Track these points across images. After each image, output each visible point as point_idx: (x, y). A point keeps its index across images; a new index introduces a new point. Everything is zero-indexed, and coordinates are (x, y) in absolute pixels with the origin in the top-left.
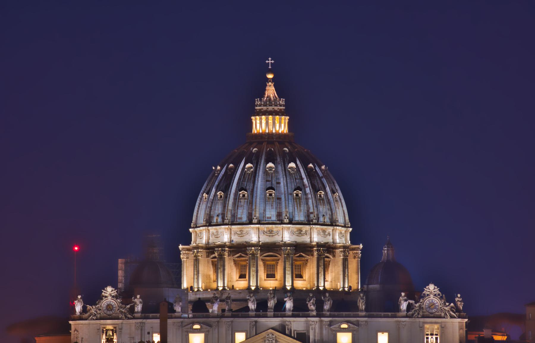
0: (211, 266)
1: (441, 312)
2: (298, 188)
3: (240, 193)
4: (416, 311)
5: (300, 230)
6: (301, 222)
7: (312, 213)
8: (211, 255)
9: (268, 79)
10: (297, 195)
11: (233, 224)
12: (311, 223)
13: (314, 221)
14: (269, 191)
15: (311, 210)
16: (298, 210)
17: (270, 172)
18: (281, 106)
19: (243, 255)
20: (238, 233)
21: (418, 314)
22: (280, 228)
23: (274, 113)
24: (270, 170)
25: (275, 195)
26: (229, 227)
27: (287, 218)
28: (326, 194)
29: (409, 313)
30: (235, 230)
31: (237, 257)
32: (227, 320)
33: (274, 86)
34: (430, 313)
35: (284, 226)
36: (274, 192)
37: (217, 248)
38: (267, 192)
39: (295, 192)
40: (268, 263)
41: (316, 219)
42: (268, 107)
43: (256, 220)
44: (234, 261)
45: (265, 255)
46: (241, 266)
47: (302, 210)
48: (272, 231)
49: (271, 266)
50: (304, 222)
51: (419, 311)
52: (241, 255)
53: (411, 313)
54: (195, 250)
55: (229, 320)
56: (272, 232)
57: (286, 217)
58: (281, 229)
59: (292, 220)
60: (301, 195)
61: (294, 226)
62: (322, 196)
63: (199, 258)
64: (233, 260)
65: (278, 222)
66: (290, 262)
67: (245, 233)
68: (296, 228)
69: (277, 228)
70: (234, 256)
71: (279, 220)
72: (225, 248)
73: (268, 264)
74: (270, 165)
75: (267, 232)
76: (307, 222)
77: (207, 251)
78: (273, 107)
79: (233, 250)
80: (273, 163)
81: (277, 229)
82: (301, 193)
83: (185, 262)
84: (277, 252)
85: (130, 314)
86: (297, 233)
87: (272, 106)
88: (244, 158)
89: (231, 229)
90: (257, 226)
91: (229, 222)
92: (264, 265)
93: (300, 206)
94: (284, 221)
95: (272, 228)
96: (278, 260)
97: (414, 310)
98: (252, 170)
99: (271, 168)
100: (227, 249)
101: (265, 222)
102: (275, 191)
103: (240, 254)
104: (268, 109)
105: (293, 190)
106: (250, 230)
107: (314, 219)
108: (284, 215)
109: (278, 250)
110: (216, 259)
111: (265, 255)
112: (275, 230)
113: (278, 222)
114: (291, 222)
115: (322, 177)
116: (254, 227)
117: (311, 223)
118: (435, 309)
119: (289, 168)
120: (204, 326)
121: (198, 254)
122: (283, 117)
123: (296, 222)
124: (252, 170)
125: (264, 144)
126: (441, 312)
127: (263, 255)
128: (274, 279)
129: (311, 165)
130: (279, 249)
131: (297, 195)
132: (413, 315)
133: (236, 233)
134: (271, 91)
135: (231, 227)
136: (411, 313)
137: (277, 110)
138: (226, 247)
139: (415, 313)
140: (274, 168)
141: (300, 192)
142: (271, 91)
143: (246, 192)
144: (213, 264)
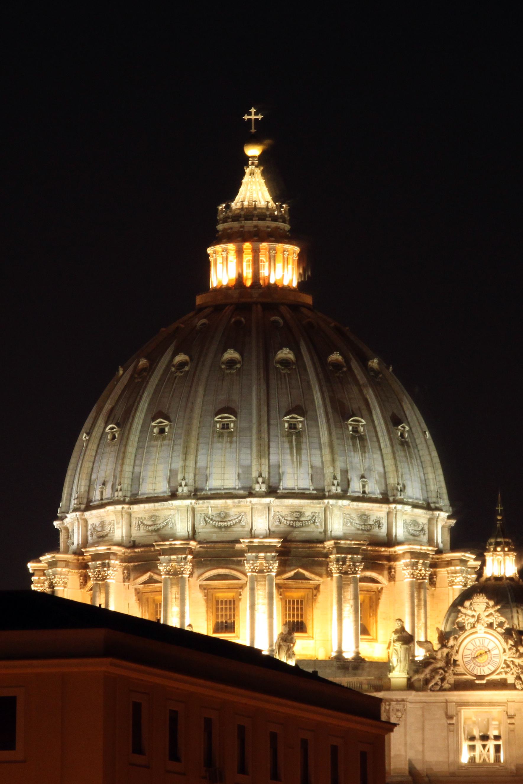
3: (153, 424)
16: (293, 463)
26: (123, 508)
31: (145, 583)
38: (216, 419)
39: (286, 418)
43: (186, 489)
48: (227, 515)
56: (225, 517)
57: (260, 480)
58: (248, 510)
64: (136, 589)
65: (242, 492)
68: (287, 506)
75: (214, 519)
86: (289, 518)
95: (227, 507)
101: (209, 493)
105: (284, 412)
106: (174, 515)
116: (180, 507)
123: (286, 491)
131: (293, 427)
133: (142, 523)
140: (239, 362)
141: (301, 419)
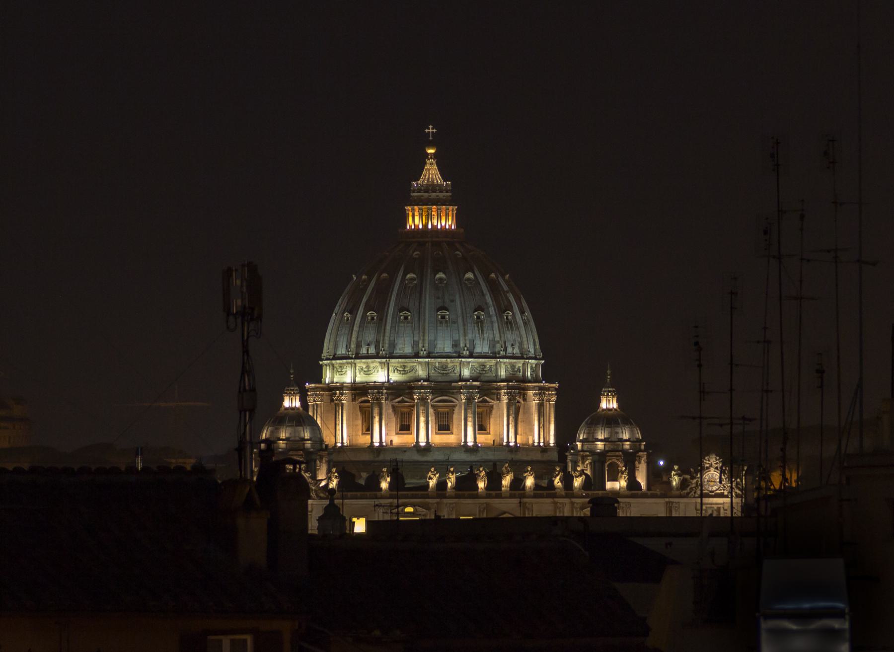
0: (359, 414)
1: (724, 490)
2: (479, 308)
3: (401, 314)
4: (692, 489)
5: (484, 365)
6: (484, 354)
7: (498, 342)
8: (359, 399)
9: (428, 154)
10: (478, 317)
11: (392, 357)
12: (498, 355)
13: (502, 352)
14: (441, 313)
15: (497, 339)
16: (480, 338)
17: (440, 285)
18: (447, 192)
19: (406, 399)
20: (398, 369)
21: (695, 493)
22: (458, 362)
23: (438, 202)
24: (441, 283)
25: (449, 317)
26: (386, 361)
27: (467, 350)
28: (514, 315)
29: (684, 492)
30: (395, 365)
31: (399, 402)
32: (449, 502)
33: (436, 164)
34: (709, 491)
35: (463, 360)
36: (448, 313)
37: (371, 390)
38: (438, 313)
39: (475, 313)
40: (440, 410)
41: (504, 351)
42: (431, 194)
43: (425, 352)
44: (393, 407)
45: (437, 399)
46: (402, 413)
47: (486, 338)
48: (447, 367)
49: (443, 415)
50: (488, 354)
51: (696, 489)
52: (403, 399)
53: (686, 491)
54: (338, 392)
55: (452, 502)
56: (446, 368)
57: (466, 348)
58: (458, 364)
59: (473, 352)
60: (484, 317)
61: (476, 360)
62: (510, 317)
63: (343, 402)
64: (392, 405)
65: (455, 354)
66: (473, 410)
67: (408, 369)
68: (478, 363)
69: (453, 363)
70: (394, 401)
71: (455, 352)
72: (382, 389)
73: (439, 411)
74: (441, 275)
75: (439, 369)
76: (491, 355)
77: (353, 392)
78: (438, 194)
79: (392, 392)
80: (444, 273)
81: (452, 364)
82: (483, 315)
83: (319, 406)
84: (453, 396)
85: (323, 493)
87: (435, 192)
88: (403, 266)
89: (388, 364)
90: (427, 360)
91: (386, 354)
92: (435, 413)
93: (483, 333)
94: (463, 353)
95: (447, 363)
96: (455, 406)
97: (689, 487)
98: (415, 282)
99: (441, 279)
100: (385, 391)
101: (437, 355)
102: (448, 311)
103: (401, 398)
104: (430, 196)
105: (473, 310)
106: (416, 366)
107: (501, 350)
108: (462, 345)
109: (454, 392)
110: (370, 404)
111: (437, 399)
112: (450, 365)
113: (455, 354)
114: (471, 356)
115: (507, 292)
116: (422, 362)
117: (498, 355)
118: (716, 486)
119: (465, 280)
120: (420, 509)
121: (342, 396)
122: (451, 208)
123: (477, 354)
124: (415, 282)
125: (427, 244)
126: (724, 490)
127: (434, 400)
128: (449, 432)
129: (493, 275)
130: (455, 391)
131: (478, 317)
132: (688, 493)
133: (396, 369)
134: (432, 173)
135: (389, 361)
136: (686, 491)
137: (442, 197)
138: (384, 388)
139: (691, 492)
140: (445, 280)
141: (483, 313)
142: (432, 173)
143: (409, 314)
144: (361, 411)
